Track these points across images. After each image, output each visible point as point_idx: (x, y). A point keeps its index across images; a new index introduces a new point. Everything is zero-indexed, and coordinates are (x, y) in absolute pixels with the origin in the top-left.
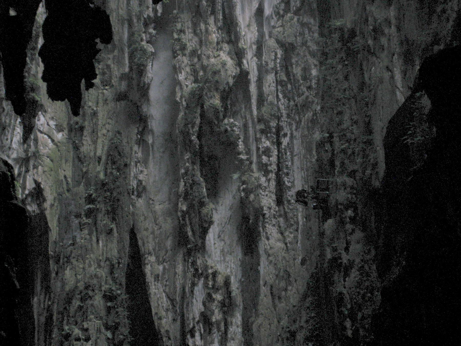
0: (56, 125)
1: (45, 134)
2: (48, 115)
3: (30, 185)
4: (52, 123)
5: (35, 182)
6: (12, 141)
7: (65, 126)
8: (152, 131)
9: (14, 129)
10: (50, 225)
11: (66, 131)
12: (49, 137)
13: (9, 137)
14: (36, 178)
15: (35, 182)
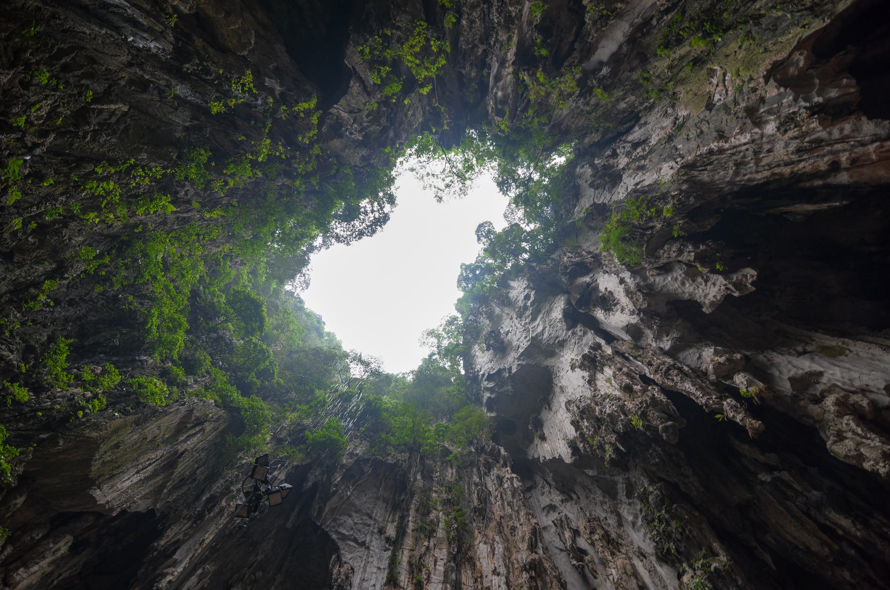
0: (712, 77)
1: (725, 86)
2: (712, 89)
3: (772, 91)
4: (715, 81)
5: (766, 83)
6: (745, 144)
7: (704, 71)
8: (631, 25)
9: (734, 147)
10: (795, 43)
11: (709, 66)
12: (724, 80)
13: (744, 148)
14: (763, 84)
15: (766, 83)
